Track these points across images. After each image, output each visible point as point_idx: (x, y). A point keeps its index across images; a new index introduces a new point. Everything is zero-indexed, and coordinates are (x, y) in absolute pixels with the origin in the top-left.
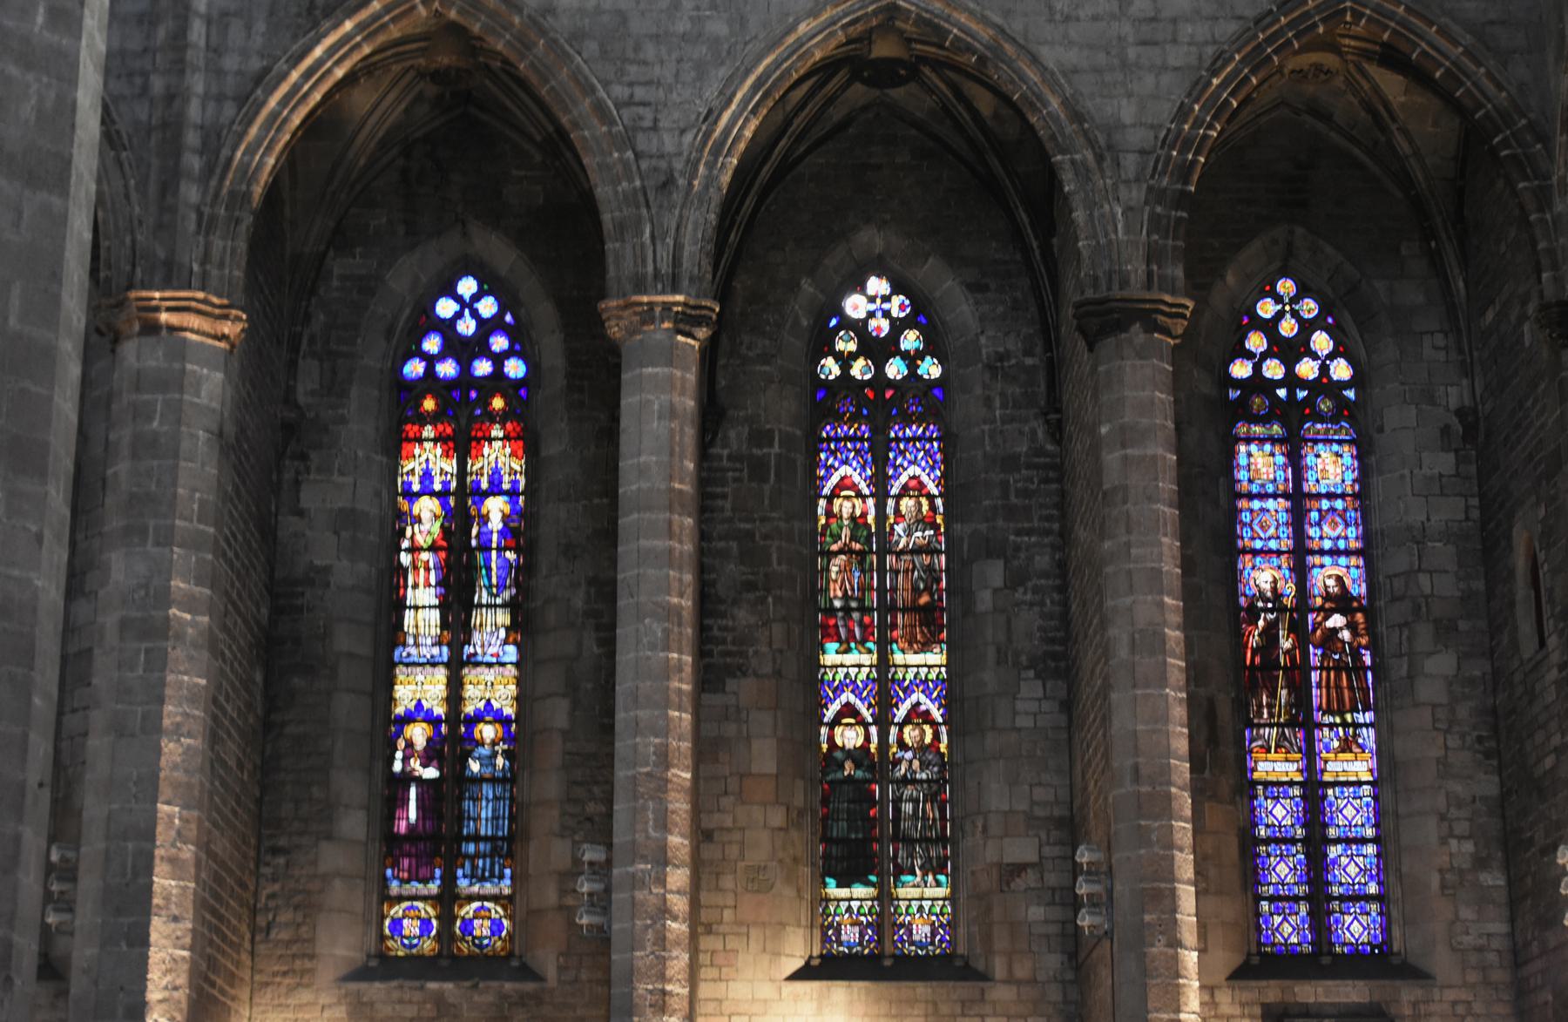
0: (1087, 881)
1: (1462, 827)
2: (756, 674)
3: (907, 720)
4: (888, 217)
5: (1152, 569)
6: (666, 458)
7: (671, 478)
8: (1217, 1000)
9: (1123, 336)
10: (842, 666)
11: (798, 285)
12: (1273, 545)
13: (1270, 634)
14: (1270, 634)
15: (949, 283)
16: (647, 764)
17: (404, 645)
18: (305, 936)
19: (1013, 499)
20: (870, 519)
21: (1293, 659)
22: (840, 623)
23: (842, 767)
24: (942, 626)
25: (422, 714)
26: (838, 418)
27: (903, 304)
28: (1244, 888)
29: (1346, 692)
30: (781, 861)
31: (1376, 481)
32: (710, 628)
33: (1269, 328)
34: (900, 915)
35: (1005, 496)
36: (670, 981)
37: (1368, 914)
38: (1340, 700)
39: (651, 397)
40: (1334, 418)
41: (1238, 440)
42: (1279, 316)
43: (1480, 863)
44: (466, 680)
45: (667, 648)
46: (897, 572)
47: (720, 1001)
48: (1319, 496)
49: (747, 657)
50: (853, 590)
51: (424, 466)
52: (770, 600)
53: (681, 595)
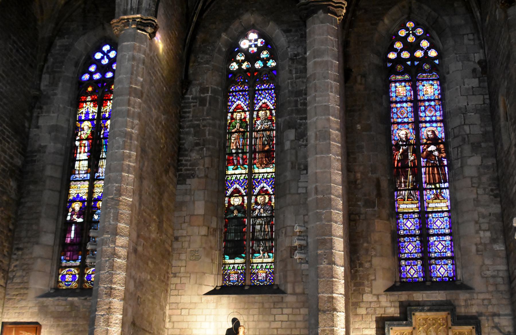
0: (298, 239)
1: (485, 226)
2: (198, 177)
3: (259, 194)
4: (254, 9)
5: (325, 105)
6: (129, 75)
7: (131, 83)
8: (380, 300)
9: (315, 15)
10: (235, 174)
11: (221, 35)
12: (406, 120)
13: (405, 154)
14: (405, 154)
15: (277, 30)
16: (112, 195)
17: (75, 174)
18: (26, 281)
19: (299, 107)
20: (247, 120)
21: (414, 163)
22: (234, 158)
23: (233, 213)
24: (273, 157)
25: (79, 199)
26: (237, 83)
27: (262, 41)
28: (394, 254)
29: (436, 176)
30: (204, 248)
31: (448, 93)
32: (182, 160)
33: (403, 40)
34: (254, 269)
35: (296, 105)
36: (115, 283)
37: (447, 264)
38: (434, 179)
39: (125, 53)
40: (430, 71)
41: (391, 82)
42: (408, 35)
43: (494, 241)
44: (95, 186)
45: (124, 148)
46: (257, 138)
47: (178, 303)
48: (424, 101)
49: (195, 171)
50: (240, 146)
51: (87, 110)
52: (205, 149)
53: (132, 128)
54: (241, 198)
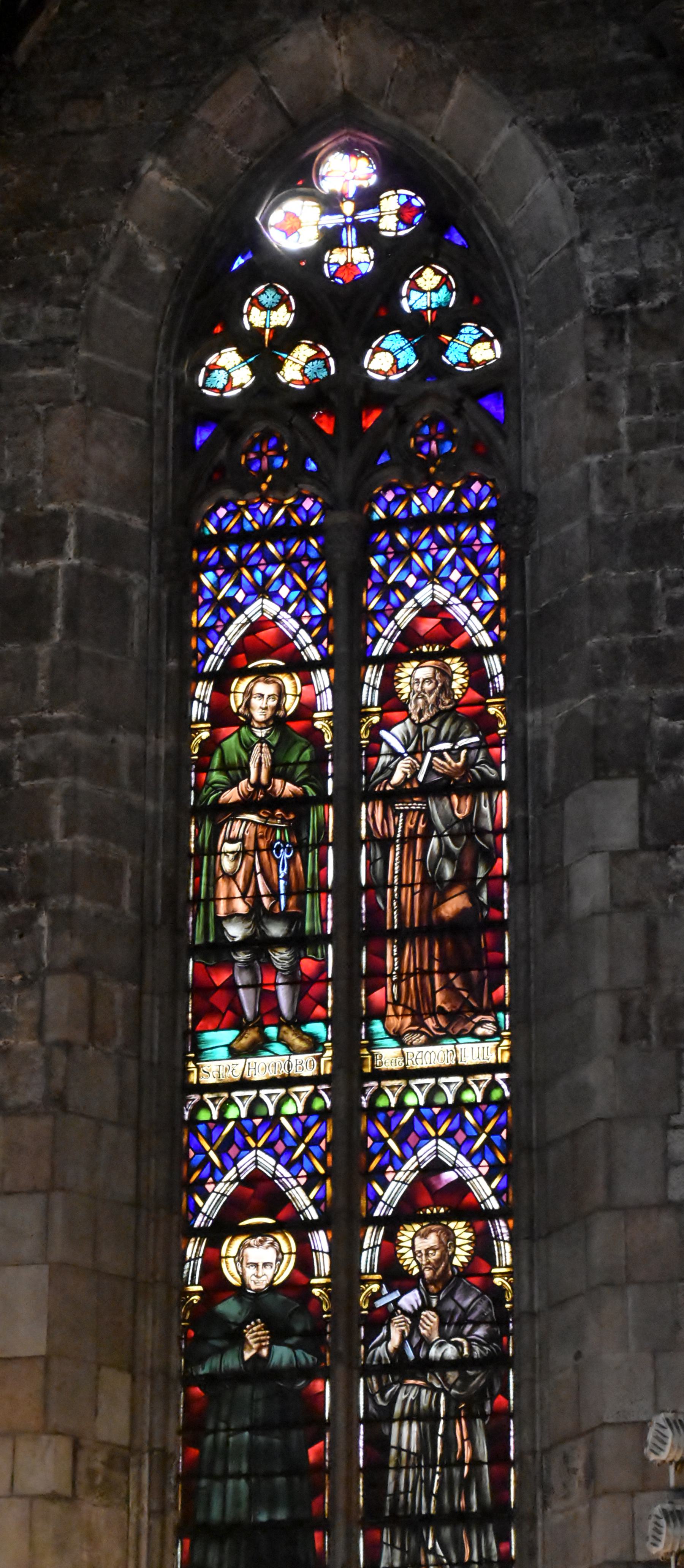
10: (244, 1084)
11: (135, 176)
15: (506, 132)
23: (238, 1340)
24: (501, 967)
27: (408, 205)
46: (386, 843)
50: (274, 894)
52: (43, 920)
54: (287, 1243)
